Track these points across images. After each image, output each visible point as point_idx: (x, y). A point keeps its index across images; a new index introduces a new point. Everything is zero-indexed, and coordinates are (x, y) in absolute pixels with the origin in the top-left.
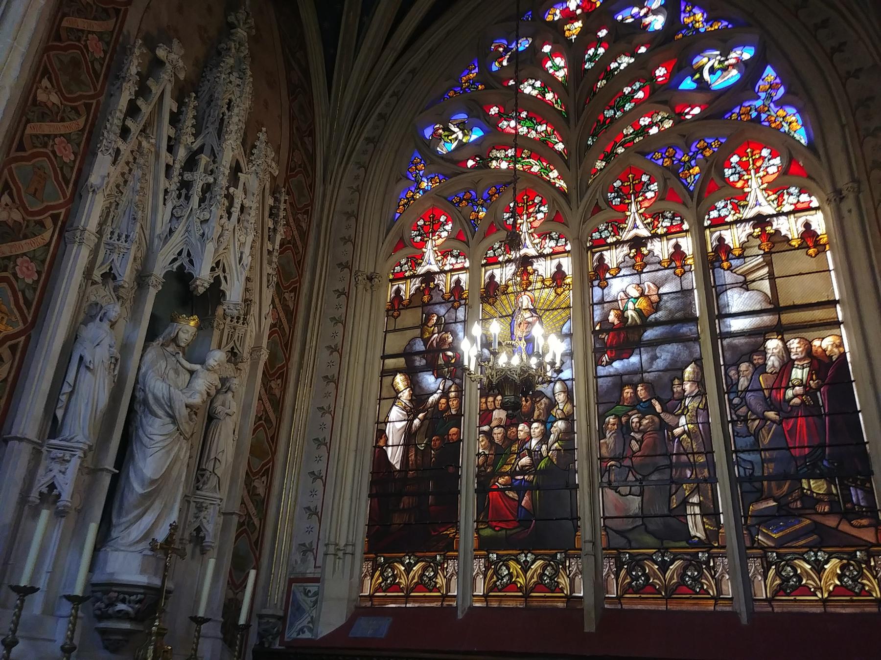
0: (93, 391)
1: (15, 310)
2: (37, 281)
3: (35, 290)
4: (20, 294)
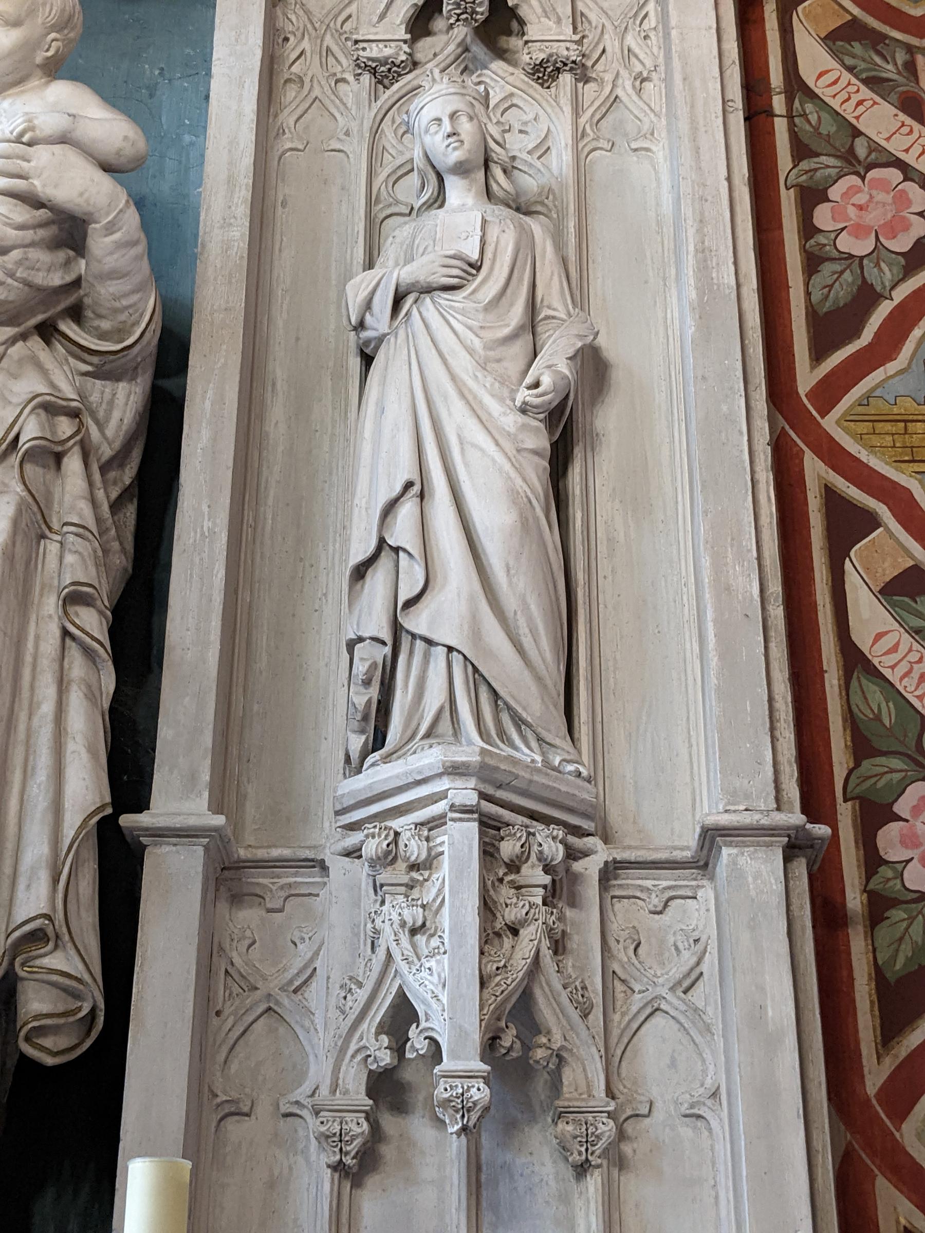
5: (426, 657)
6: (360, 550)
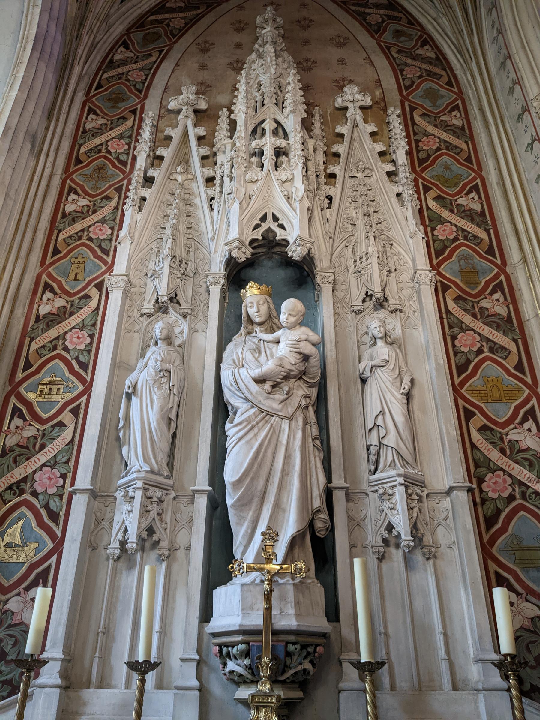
0: (145, 414)
1: (72, 377)
2: (91, 344)
3: (89, 352)
4: (74, 363)
5: (387, 449)
6: (370, 425)
